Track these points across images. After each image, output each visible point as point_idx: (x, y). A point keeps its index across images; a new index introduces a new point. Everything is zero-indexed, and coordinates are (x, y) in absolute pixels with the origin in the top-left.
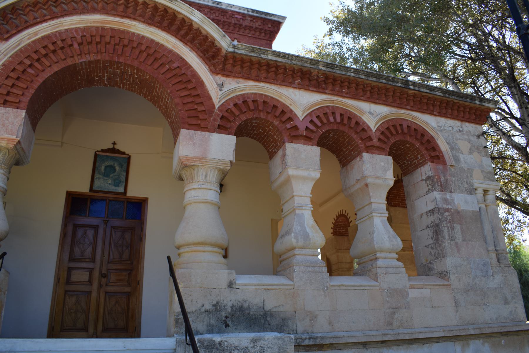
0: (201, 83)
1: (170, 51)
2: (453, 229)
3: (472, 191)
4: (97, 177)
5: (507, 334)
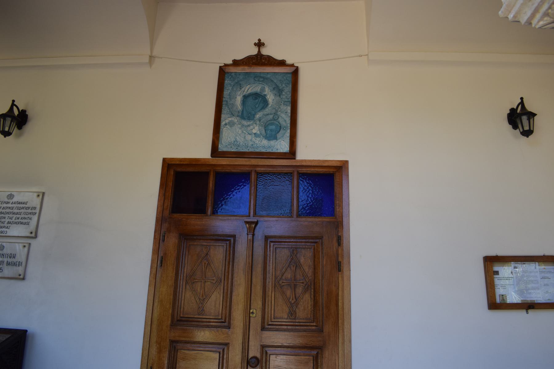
4: (227, 121)
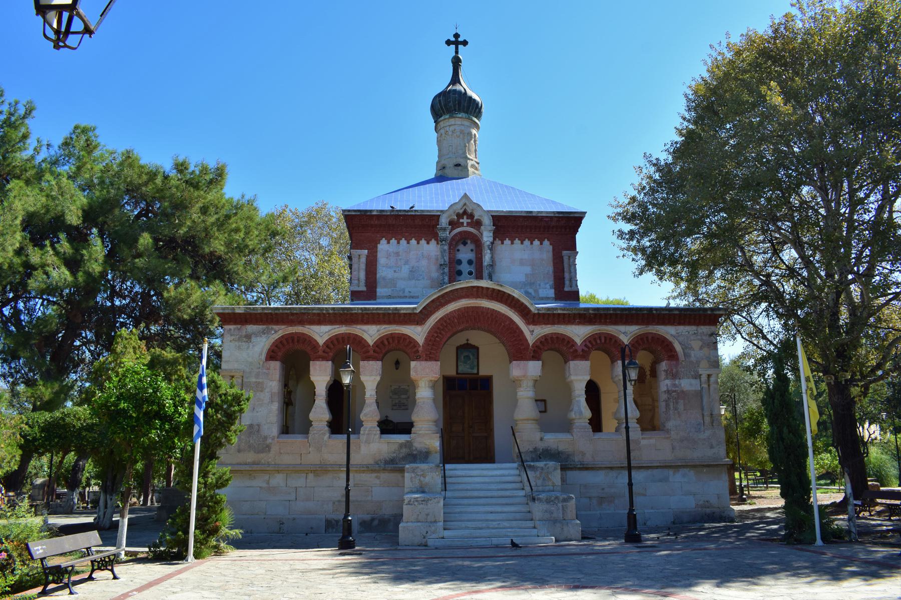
0: (522, 332)
1: (504, 315)
2: (677, 403)
3: (698, 376)
5: (708, 466)
